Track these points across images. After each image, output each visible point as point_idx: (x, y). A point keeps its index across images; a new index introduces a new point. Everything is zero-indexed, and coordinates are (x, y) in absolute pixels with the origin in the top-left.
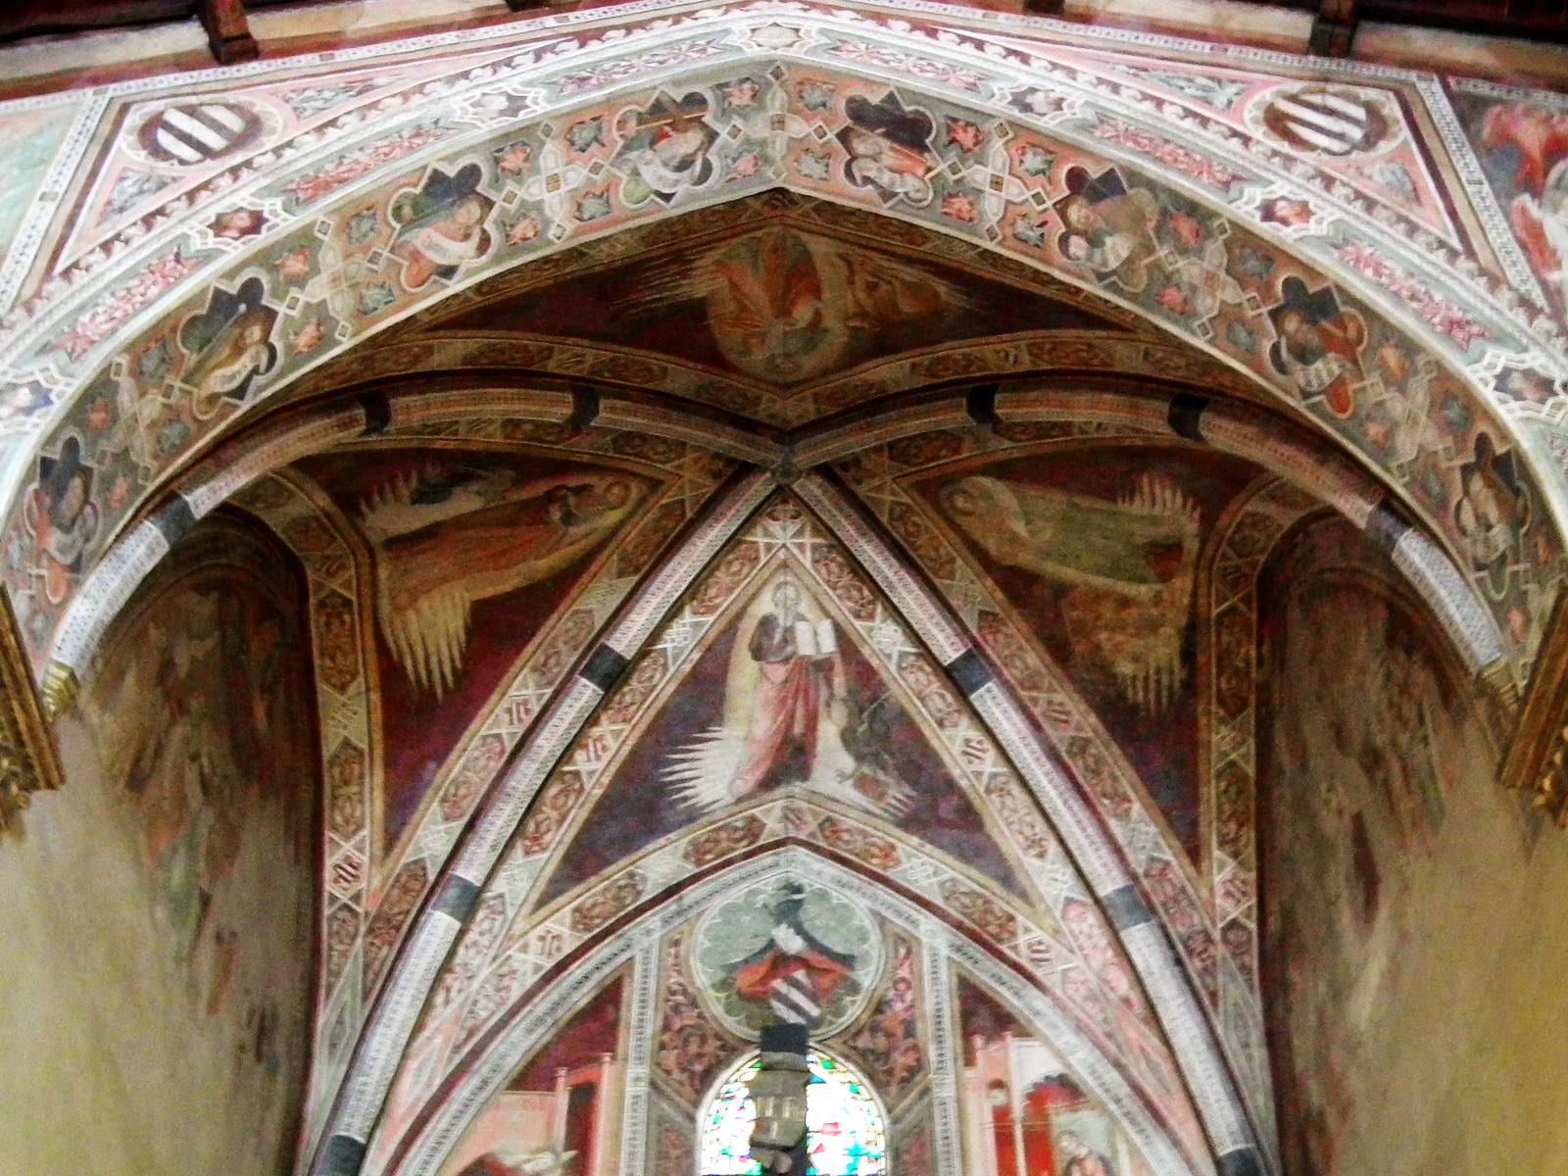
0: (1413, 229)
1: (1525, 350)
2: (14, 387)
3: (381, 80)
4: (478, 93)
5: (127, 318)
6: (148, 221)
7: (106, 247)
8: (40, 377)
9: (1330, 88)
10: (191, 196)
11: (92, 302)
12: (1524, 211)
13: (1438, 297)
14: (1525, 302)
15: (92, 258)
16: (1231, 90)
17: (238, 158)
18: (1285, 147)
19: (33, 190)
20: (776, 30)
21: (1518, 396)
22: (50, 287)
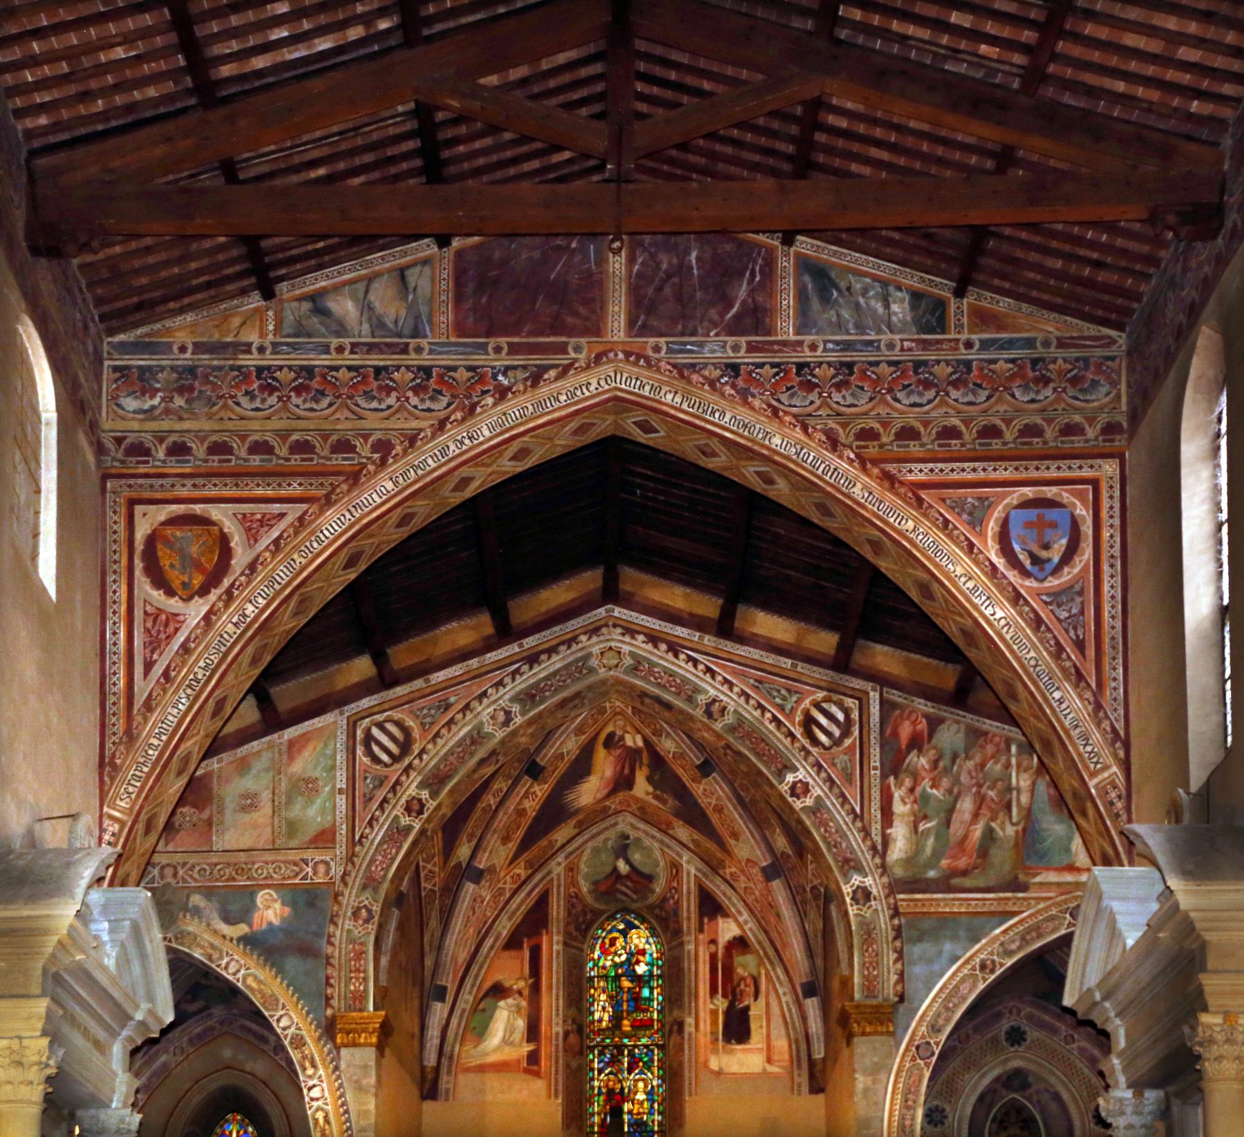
0: (844, 800)
1: (866, 876)
2: (359, 909)
3: (452, 699)
4: (491, 709)
5: (390, 866)
6: (381, 807)
7: (370, 824)
8: (366, 902)
9: (835, 697)
10: (393, 789)
11: (372, 861)
12: (889, 787)
13: (844, 845)
14: (873, 848)
15: (367, 831)
16: (794, 698)
17: (407, 762)
18: (806, 742)
19: (334, 787)
20: (611, 654)
21: (857, 903)
22: (357, 849)
